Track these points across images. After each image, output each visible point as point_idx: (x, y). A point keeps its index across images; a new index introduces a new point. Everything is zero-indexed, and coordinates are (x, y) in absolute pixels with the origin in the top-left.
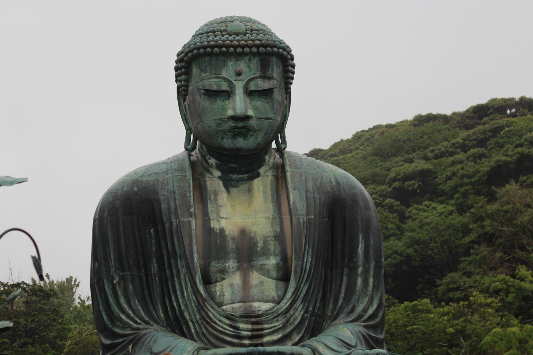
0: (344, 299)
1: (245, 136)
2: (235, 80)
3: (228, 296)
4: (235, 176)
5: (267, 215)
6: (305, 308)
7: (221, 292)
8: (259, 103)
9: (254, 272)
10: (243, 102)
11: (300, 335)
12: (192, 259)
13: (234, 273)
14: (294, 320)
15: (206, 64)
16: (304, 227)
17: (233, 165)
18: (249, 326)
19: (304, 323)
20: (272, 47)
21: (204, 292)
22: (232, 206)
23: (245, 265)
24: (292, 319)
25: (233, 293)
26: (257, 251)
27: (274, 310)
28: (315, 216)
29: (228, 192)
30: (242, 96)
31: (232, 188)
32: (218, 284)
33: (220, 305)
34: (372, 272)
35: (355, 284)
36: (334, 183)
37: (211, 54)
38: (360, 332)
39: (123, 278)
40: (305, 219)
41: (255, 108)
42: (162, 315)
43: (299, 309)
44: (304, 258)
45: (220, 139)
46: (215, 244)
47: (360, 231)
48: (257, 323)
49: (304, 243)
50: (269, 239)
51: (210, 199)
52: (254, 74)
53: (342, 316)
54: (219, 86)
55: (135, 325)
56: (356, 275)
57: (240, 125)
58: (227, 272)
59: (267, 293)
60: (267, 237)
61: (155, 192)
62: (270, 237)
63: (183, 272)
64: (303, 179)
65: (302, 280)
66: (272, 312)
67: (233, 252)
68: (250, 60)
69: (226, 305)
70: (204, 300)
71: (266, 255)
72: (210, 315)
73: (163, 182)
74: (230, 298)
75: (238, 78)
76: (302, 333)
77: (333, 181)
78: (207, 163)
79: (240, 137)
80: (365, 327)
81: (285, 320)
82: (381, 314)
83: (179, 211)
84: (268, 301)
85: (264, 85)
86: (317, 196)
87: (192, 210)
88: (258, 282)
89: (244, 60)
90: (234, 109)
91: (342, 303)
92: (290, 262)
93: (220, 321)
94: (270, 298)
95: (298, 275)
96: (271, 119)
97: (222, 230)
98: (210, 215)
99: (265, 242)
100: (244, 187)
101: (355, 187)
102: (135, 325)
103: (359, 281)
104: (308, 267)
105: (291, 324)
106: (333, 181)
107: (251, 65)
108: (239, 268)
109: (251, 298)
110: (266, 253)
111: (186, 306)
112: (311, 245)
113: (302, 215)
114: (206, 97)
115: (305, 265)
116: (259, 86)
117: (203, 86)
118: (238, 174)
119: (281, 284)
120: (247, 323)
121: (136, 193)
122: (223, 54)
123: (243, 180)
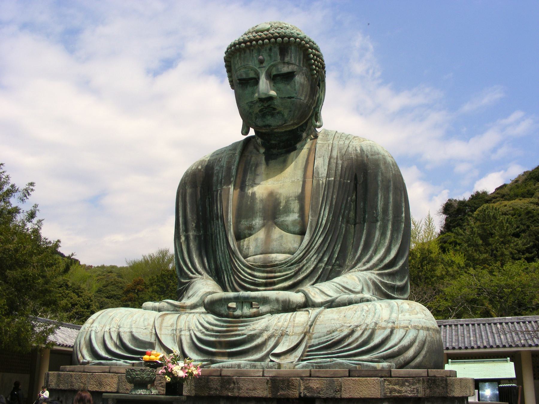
1: (273, 115)
2: (259, 68)
3: (252, 249)
4: (275, 151)
5: (293, 179)
6: (319, 258)
7: (247, 246)
8: (281, 86)
9: (277, 227)
10: (264, 85)
11: (312, 282)
12: (227, 219)
13: (259, 229)
14: (307, 268)
15: (238, 58)
16: (322, 187)
17: (273, 142)
18: (265, 275)
19: (318, 271)
20: (289, 37)
21: (234, 246)
22: (267, 174)
23: (270, 223)
24: (305, 268)
25: (257, 246)
26: (280, 210)
27: (287, 260)
28: (335, 178)
29: (267, 164)
30: (265, 80)
31: (272, 159)
32: (246, 239)
33: (245, 257)
34: (390, 227)
35: (374, 237)
36: (359, 151)
38: (370, 279)
40: (324, 181)
41: (277, 90)
42: (213, 267)
43: (313, 259)
44: (320, 214)
45: (254, 119)
47: (379, 190)
48: (271, 272)
49: (321, 201)
50: (291, 199)
51: (251, 170)
52: (275, 61)
53: (359, 265)
54: (247, 74)
55: (191, 275)
57: (266, 105)
58: (254, 229)
59: (284, 246)
60: (289, 198)
61: (213, 168)
62: (291, 197)
64: (330, 148)
65: (318, 233)
66: (286, 262)
67: (260, 212)
68: (270, 49)
69: (250, 256)
70: (234, 253)
71: (286, 213)
72: (237, 265)
73: (219, 160)
74: (254, 250)
75: (261, 66)
76: (314, 281)
77: (358, 149)
78: (257, 143)
79: (268, 115)
80: (379, 275)
81: (297, 268)
82: (401, 263)
83: (223, 180)
84: (284, 253)
86: (340, 162)
87: (232, 179)
88: (278, 236)
89: (266, 50)
90: (259, 92)
91: (361, 254)
92: (307, 218)
93: (243, 270)
94: (287, 250)
95: (313, 229)
96: (293, 98)
97: (254, 194)
98: (247, 183)
99: (287, 201)
100: (281, 159)
101: (378, 154)
102: (191, 275)
104: (324, 222)
105: (304, 272)
106: (358, 149)
107: (272, 54)
108: (264, 225)
109: (270, 250)
110: (287, 211)
111: (223, 258)
112: (329, 202)
113: (322, 177)
114: (241, 86)
115: (320, 220)
116: (280, 70)
117: (237, 76)
118: (278, 149)
119: (298, 237)
120: (263, 272)
121: (200, 170)
123: (282, 154)
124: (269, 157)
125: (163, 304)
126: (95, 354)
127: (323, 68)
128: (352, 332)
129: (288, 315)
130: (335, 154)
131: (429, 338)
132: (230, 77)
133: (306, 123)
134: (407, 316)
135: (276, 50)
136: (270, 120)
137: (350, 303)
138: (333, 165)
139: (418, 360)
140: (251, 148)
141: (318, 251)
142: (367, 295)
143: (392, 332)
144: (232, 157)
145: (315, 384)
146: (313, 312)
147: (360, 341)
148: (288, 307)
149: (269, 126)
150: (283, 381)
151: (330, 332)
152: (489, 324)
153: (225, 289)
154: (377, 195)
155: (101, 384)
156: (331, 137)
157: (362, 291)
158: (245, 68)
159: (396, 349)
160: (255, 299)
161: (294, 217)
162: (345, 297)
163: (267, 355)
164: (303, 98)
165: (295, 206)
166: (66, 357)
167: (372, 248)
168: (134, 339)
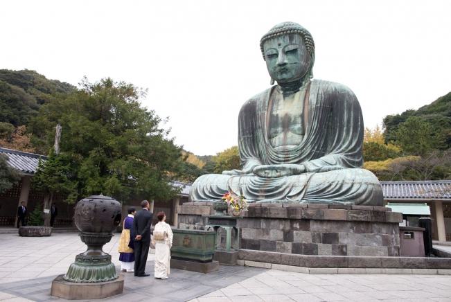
0: (337, 142)
1: (286, 73)
3: (277, 143)
4: (288, 92)
25: (279, 142)
33: (274, 147)
34: (351, 130)
37: (268, 39)
39: (244, 139)
46: (274, 122)
53: (335, 150)
56: (343, 130)
57: (282, 68)
61: (256, 103)
63: (262, 136)
82: (358, 149)
85: (291, 47)
86: (323, 96)
97: (277, 115)
100: (291, 96)
103: (344, 133)
108: (283, 131)
110: (295, 123)
119: (301, 137)
122: (273, 38)
124: (285, 95)
125: (232, 172)
126: (199, 197)
127: (314, 45)
128: (330, 185)
129: (296, 176)
130: (320, 92)
131: (374, 190)
132: (263, 54)
133: (304, 77)
134: (361, 177)
135: (287, 38)
136: (285, 76)
137: (329, 170)
138: (319, 98)
139: (368, 201)
140: (275, 91)
141: (311, 144)
142: (338, 166)
143: (352, 185)
144: (266, 96)
145: (310, 212)
146: (309, 175)
147: (335, 190)
148: (296, 172)
149: (284, 79)
150: (293, 210)
151: (318, 185)
152: (414, 185)
153: (263, 164)
154: (344, 112)
155: (201, 211)
156: (318, 83)
157: (336, 164)
158: (271, 49)
159: (355, 194)
160: (278, 168)
161: (299, 126)
162: (327, 167)
163: (285, 197)
164: (302, 63)
165: (299, 120)
166: (186, 199)
167: (341, 142)
168: (218, 189)
